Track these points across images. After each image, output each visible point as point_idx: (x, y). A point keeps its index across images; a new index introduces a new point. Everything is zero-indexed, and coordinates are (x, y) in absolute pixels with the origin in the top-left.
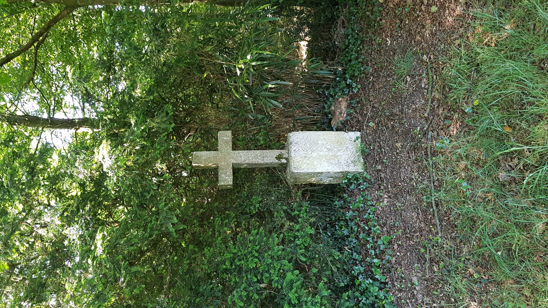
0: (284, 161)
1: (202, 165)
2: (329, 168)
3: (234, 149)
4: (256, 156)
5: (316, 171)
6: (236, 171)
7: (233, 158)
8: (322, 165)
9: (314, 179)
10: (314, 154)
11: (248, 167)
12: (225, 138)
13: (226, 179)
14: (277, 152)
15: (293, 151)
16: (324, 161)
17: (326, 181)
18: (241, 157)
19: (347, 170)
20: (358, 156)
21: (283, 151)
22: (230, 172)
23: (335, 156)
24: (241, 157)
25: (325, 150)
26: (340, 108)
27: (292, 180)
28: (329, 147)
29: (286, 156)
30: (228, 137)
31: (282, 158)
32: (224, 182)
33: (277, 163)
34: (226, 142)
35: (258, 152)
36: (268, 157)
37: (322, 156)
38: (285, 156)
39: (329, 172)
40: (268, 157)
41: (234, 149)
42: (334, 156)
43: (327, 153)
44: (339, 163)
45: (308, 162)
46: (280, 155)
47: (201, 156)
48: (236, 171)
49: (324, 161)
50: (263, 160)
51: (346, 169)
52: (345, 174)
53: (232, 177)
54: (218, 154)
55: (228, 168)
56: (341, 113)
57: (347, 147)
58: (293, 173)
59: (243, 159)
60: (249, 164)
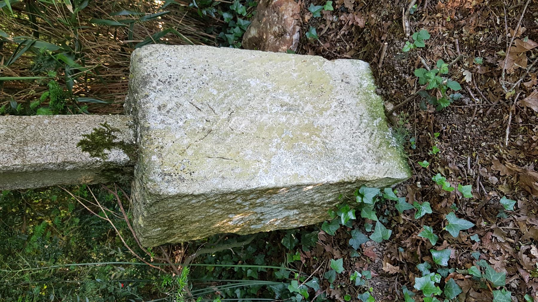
0: (116, 156)
2: (302, 170)
5: (254, 185)
8: (274, 161)
9: (238, 217)
10: (241, 123)
14: (86, 124)
15: (153, 110)
16: (278, 147)
17: (274, 220)
19: (358, 174)
20: (380, 127)
21: (114, 121)
23: (313, 130)
25: (276, 109)
26: (281, 19)
27: (156, 231)
28: (286, 99)
29: (126, 135)
31: (110, 145)
33: (87, 168)
37: (271, 129)
38: (120, 138)
39: (299, 187)
42: (307, 128)
43: (284, 119)
44: (328, 153)
45: (222, 150)
46: (99, 133)
49: (278, 147)
50: (22, 154)
51: (350, 172)
52: (348, 193)
56: (280, 35)
57: (341, 103)
58: (160, 199)
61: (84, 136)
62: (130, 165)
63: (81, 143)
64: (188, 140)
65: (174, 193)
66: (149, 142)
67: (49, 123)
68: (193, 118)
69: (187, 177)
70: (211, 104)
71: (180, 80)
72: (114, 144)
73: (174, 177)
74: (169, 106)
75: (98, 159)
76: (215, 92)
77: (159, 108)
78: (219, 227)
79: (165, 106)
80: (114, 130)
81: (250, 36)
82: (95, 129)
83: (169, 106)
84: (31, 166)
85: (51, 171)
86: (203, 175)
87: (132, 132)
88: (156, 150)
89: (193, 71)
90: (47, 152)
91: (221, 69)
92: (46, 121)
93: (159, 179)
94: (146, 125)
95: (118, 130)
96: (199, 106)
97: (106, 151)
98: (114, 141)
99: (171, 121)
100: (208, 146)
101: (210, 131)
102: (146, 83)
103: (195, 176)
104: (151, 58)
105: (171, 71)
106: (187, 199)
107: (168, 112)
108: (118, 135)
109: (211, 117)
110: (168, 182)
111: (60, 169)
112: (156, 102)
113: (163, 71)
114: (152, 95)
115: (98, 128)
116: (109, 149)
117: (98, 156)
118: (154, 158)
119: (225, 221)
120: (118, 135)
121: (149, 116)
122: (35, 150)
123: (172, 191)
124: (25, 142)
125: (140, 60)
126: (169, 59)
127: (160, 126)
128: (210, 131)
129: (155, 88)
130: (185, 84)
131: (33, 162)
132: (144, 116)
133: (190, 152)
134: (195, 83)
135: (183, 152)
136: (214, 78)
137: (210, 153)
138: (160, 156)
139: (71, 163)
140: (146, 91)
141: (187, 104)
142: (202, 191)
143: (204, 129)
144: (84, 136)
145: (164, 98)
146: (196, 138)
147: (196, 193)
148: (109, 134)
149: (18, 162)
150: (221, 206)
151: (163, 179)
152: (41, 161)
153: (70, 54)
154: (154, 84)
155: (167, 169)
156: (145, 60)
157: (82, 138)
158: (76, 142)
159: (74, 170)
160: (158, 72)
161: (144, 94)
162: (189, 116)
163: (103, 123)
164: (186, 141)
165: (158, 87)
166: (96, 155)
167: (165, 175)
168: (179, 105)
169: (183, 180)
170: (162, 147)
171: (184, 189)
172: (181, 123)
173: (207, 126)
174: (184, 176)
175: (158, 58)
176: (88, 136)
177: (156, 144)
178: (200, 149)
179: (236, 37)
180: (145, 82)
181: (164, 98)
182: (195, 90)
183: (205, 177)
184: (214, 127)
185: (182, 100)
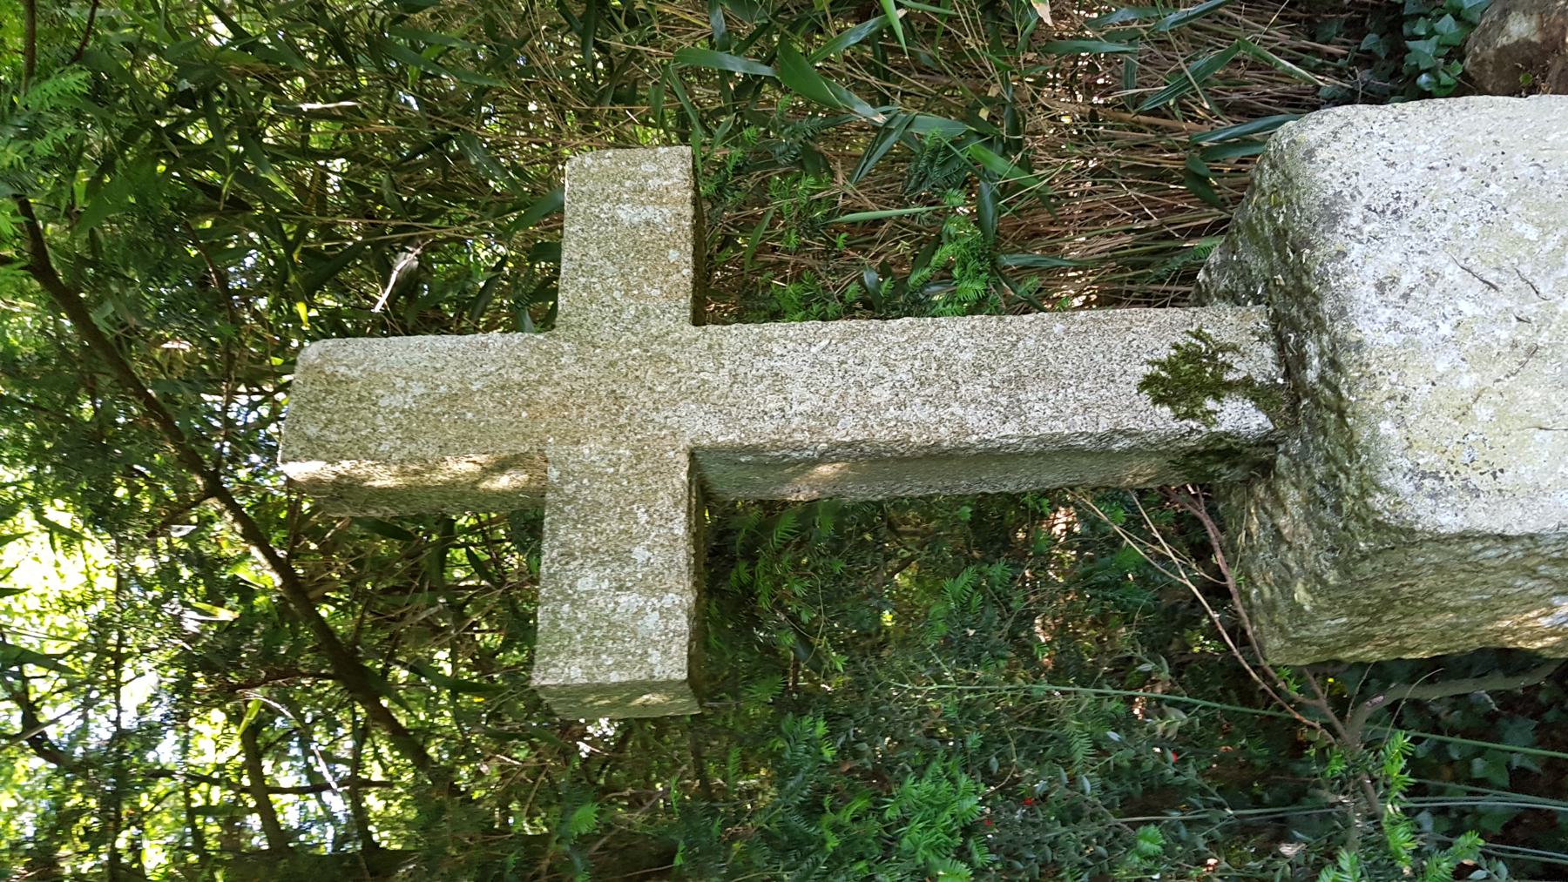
0: (1238, 417)
1: (384, 478)
3: (698, 319)
4: (939, 379)
6: (743, 538)
7: (700, 393)
11: (857, 493)
12: (625, 213)
13: (621, 621)
14: (1155, 333)
15: (1365, 293)
18: (779, 381)
22: (663, 538)
24: (779, 381)
30: (659, 198)
31: (1219, 389)
32: (592, 649)
34: (639, 247)
35: (956, 336)
36: (1059, 380)
40: (1059, 380)
41: (698, 319)
46: (1189, 355)
47: (372, 379)
48: (743, 538)
50: (1015, 410)
53: (679, 597)
54: (553, 357)
55: (647, 499)
59: (802, 399)
60: (870, 459)
61: (1152, 363)
62: (1268, 442)
63: (1148, 383)
64: (1475, 376)
65: (1455, 529)
66: (1365, 382)
67: (1067, 332)
68: (1479, 311)
69: (1485, 482)
70: (1526, 269)
71: (1424, 204)
72: (1230, 386)
73: (1448, 482)
74: (1406, 281)
75: (1194, 424)
76: (1532, 233)
77: (1381, 287)
78: (1503, 632)
79: (1395, 281)
80: (1223, 349)
81: (1503, 41)
82: (1176, 347)
83: (1406, 281)
84: (1040, 440)
85: (1081, 452)
86: (1528, 479)
87: (1269, 353)
88: (1388, 406)
89: (1457, 175)
90: (1072, 405)
91: (1540, 162)
92: (1058, 328)
93: (1406, 487)
94: (1353, 337)
95: (1234, 349)
96: (1492, 277)
97: (1210, 404)
98: (1229, 377)
99: (1416, 322)
100: (1532, 394)
101: (1532, 351)
102: (1334, 219)
103: (1505, 480)
104: (1335, 145)
105: (1397, 180)
106: (1478, 546)
107: (1406, 297)
108: (1236, 361)
109: (1530, 309)
110: (1434, 495)
111: (1101, 450)
112: (1369, 270)
113: (1376, 180)
114: (1356, 251)
115: (1182, 343)
116: (1217, 398)
117: (1193, 417)
118: (1386, 427)
119: (1535, 613)
120: (1236, 361)
121: (1355, 310)
122: (1044, 400)
123: (1449, 521)
124: (1019, 381)
125: (1310, 154)
126: (1385, 143)
127: (1390, 339)
128: (1532, 351)
129: (1358, 229)
130: (1441, 214)
131: (1044, 430)
132: (1343, 312)
133: (1482, 412)
134: (1469, 208)
135: (1464, 413)
136: (1524, 191)
137: (1543, 416)
138: (1401, 423)
139: (1126, 434)
140: (1338, 242)
141: (1452, 273)
142: (1531, 527)
143: (1515, 345)
144: (1152, 363)
145: (1389, 258)
146: (1496, 371)
147: (1510, 532)
148: (1213, 357)
149: (1011, 429)
150: (1556, 571)
151: (1418, 488)
152: (1061, 427)
153: (989, 144)
154: (1355, 221)
155: (1427, 460)
156: (1322, 154)
157: (1147, 370)
158: (1135, 381)
159: (1130, 450)
160: (1362, 184)
161: (1333, 250)
162: (1464, 306)
163: (1193, 329)
164: (1468, 381)
165: (1367, 228)
166: (1187, 415)
167: (1424, 475)
168: (1432, 277)
169: (1476, 493)
170: (1405, 399)
171: (1481, 518)
172: (1445, 329)
173: (1525, 335)
174: (1475, 480)
175: (1358, 146)
176: (1162, 365)
177: (1386, 387)
178: (1513, 401)
179: (1439, 46)
180: (1332, 215)
181: (1389, 258)
182: (1474, 229)
183: (1537, 487)
184: (1543, 338)
185: (1440, 260)
